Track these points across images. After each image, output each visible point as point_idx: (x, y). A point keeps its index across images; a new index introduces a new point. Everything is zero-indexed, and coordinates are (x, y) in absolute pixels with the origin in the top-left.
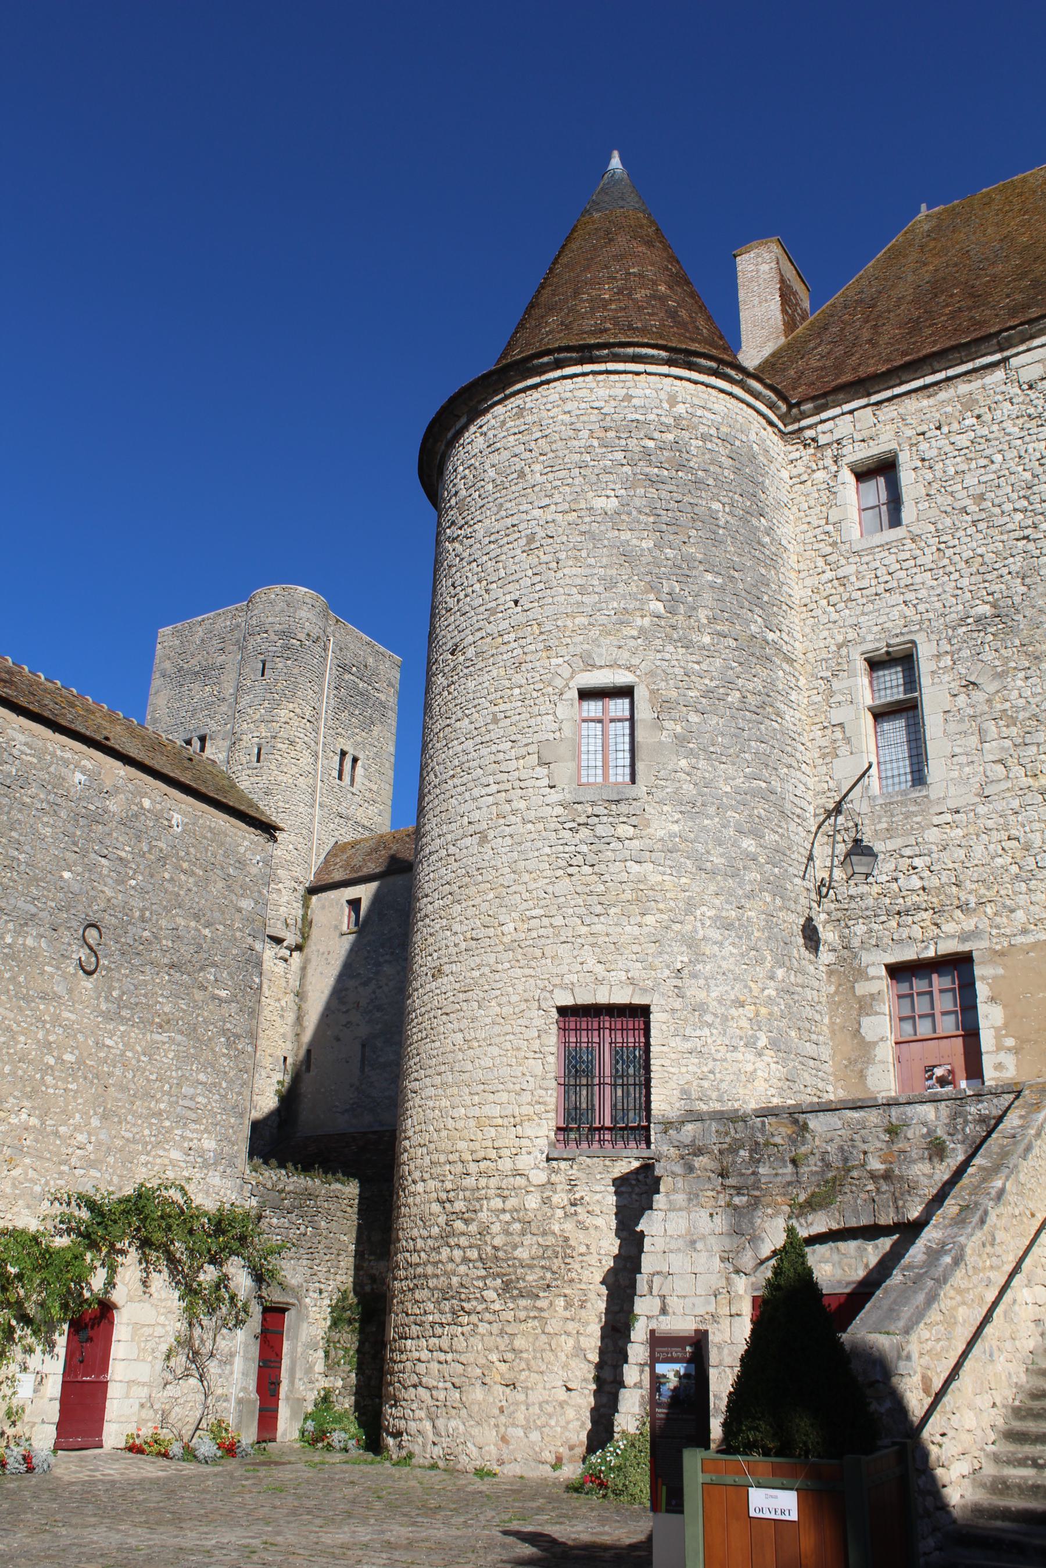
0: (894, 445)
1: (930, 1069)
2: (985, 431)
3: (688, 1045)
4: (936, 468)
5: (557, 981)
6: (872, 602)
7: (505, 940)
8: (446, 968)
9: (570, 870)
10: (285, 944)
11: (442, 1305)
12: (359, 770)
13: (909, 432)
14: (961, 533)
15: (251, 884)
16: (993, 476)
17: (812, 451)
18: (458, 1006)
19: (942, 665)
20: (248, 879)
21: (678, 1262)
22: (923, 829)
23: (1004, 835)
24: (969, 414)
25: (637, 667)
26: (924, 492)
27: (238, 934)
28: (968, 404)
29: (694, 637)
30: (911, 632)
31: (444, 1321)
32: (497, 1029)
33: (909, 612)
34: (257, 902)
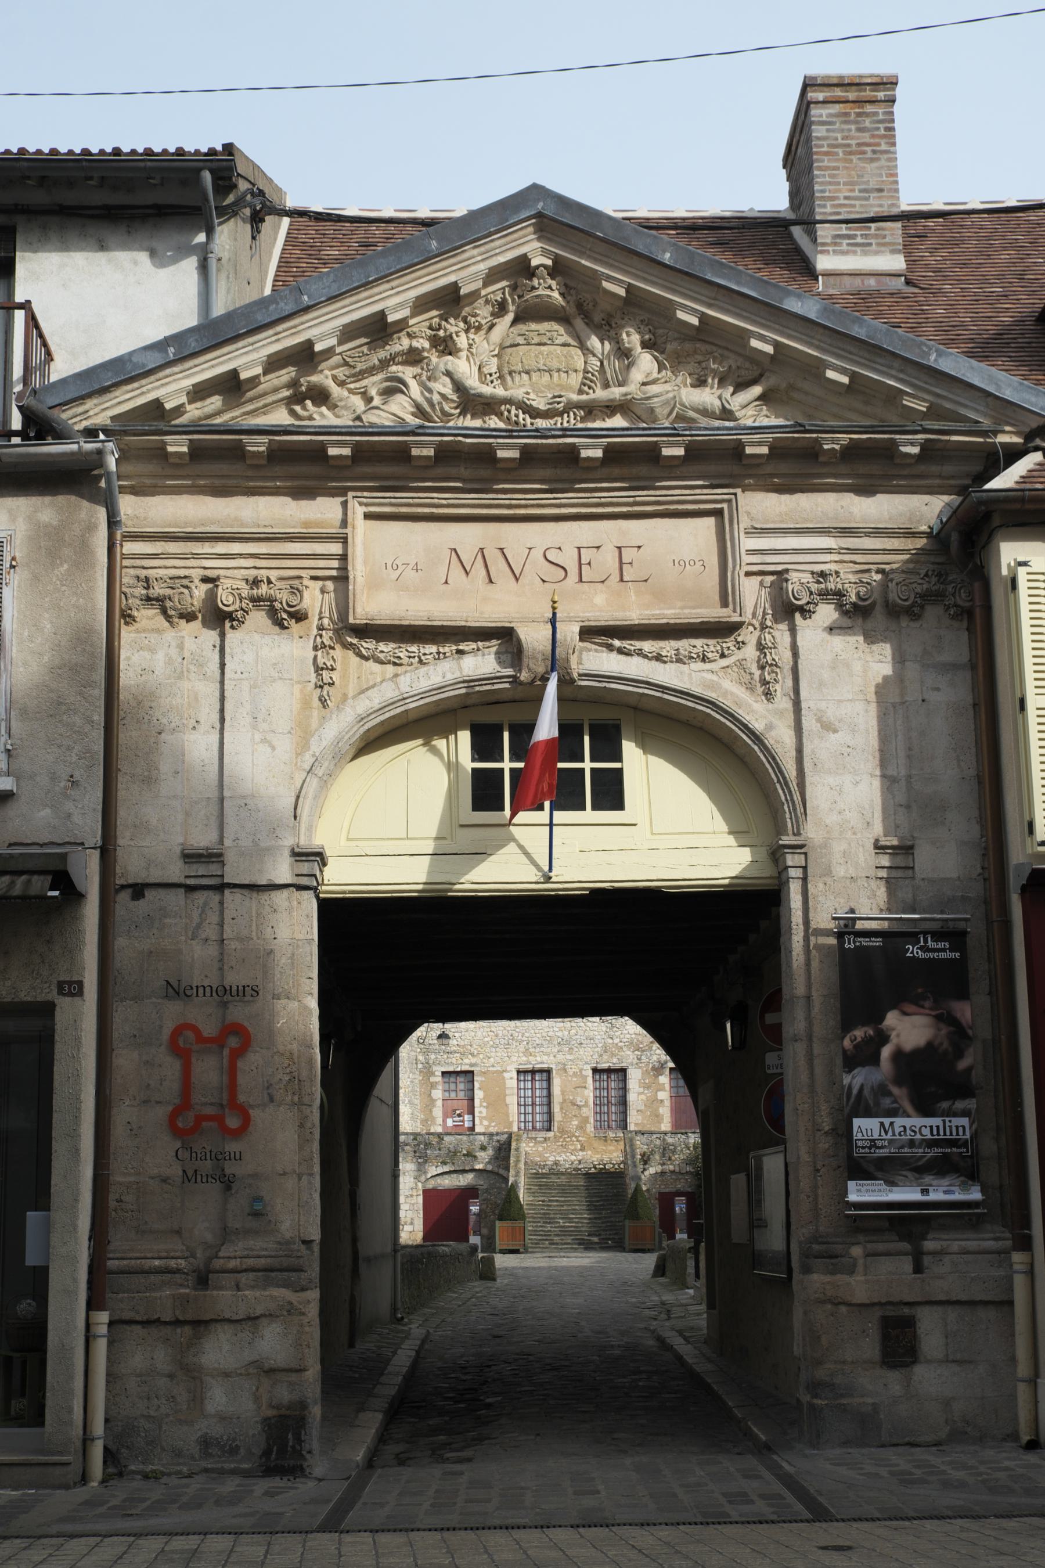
1: (455, 1111)
23: (489, 1030)
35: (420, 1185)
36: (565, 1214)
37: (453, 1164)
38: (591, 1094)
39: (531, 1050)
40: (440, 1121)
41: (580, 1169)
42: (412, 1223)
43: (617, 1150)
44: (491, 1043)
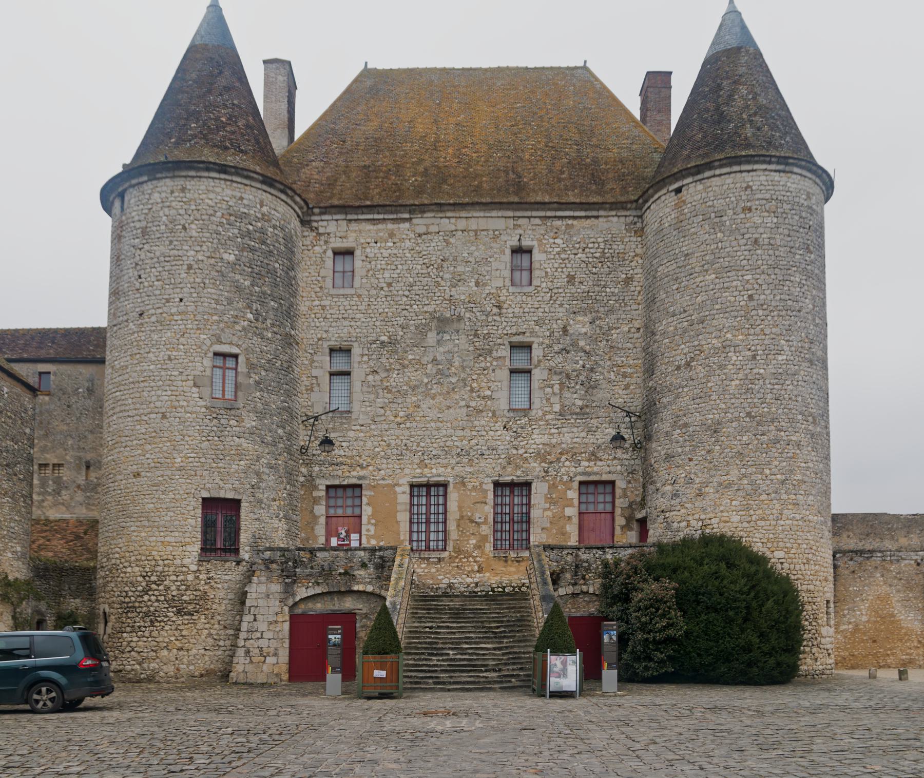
0: (353, 245)
2: (396, 251)
3: (256, 517)
4: (372, 263)
5: (202, 486)
6: (336, 322)
7: (176, 465)
8: (143, 474)
9: (209, 438)
13: (362, 241)
14: (379, 299)
16: (396, 276)
17: (315, 234)
19: (364, 359)
21: (261, 603)
22: (348, 430)
23: (380, 439)
24: (390, 240)
25: (241, 346)
26: (365, 274)
28: (392, 235)
29: (265, 333)
30: (351, 341)
32: (173, 505)
33: (352, 331)
35: (286, 609)
36: (457, 643)
37: (327, 584)
38: (492, 511)
39: (426, 461)
40: (322, 540)
41: (476, 593)
42: (275, 655)
43: (518, 572)
44: (383, 453)
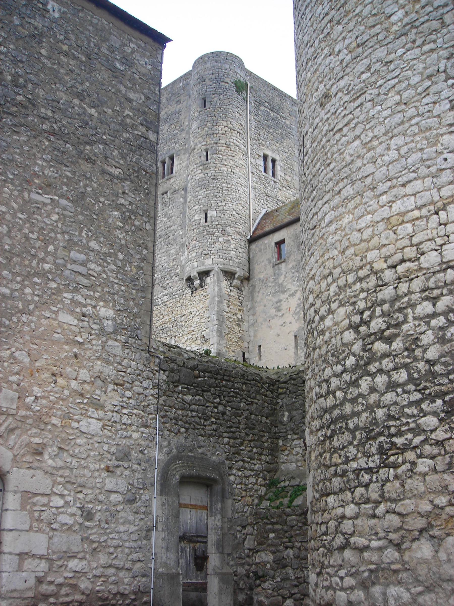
10: (236, 276)
11: (367, 446)
12: (278, 168)
15: (140, 81)
18: (351, 116)
20: (138, 77)
27: (128, 120)
31: (371, 465)
32: (398, 117)
34: (148, 98)
